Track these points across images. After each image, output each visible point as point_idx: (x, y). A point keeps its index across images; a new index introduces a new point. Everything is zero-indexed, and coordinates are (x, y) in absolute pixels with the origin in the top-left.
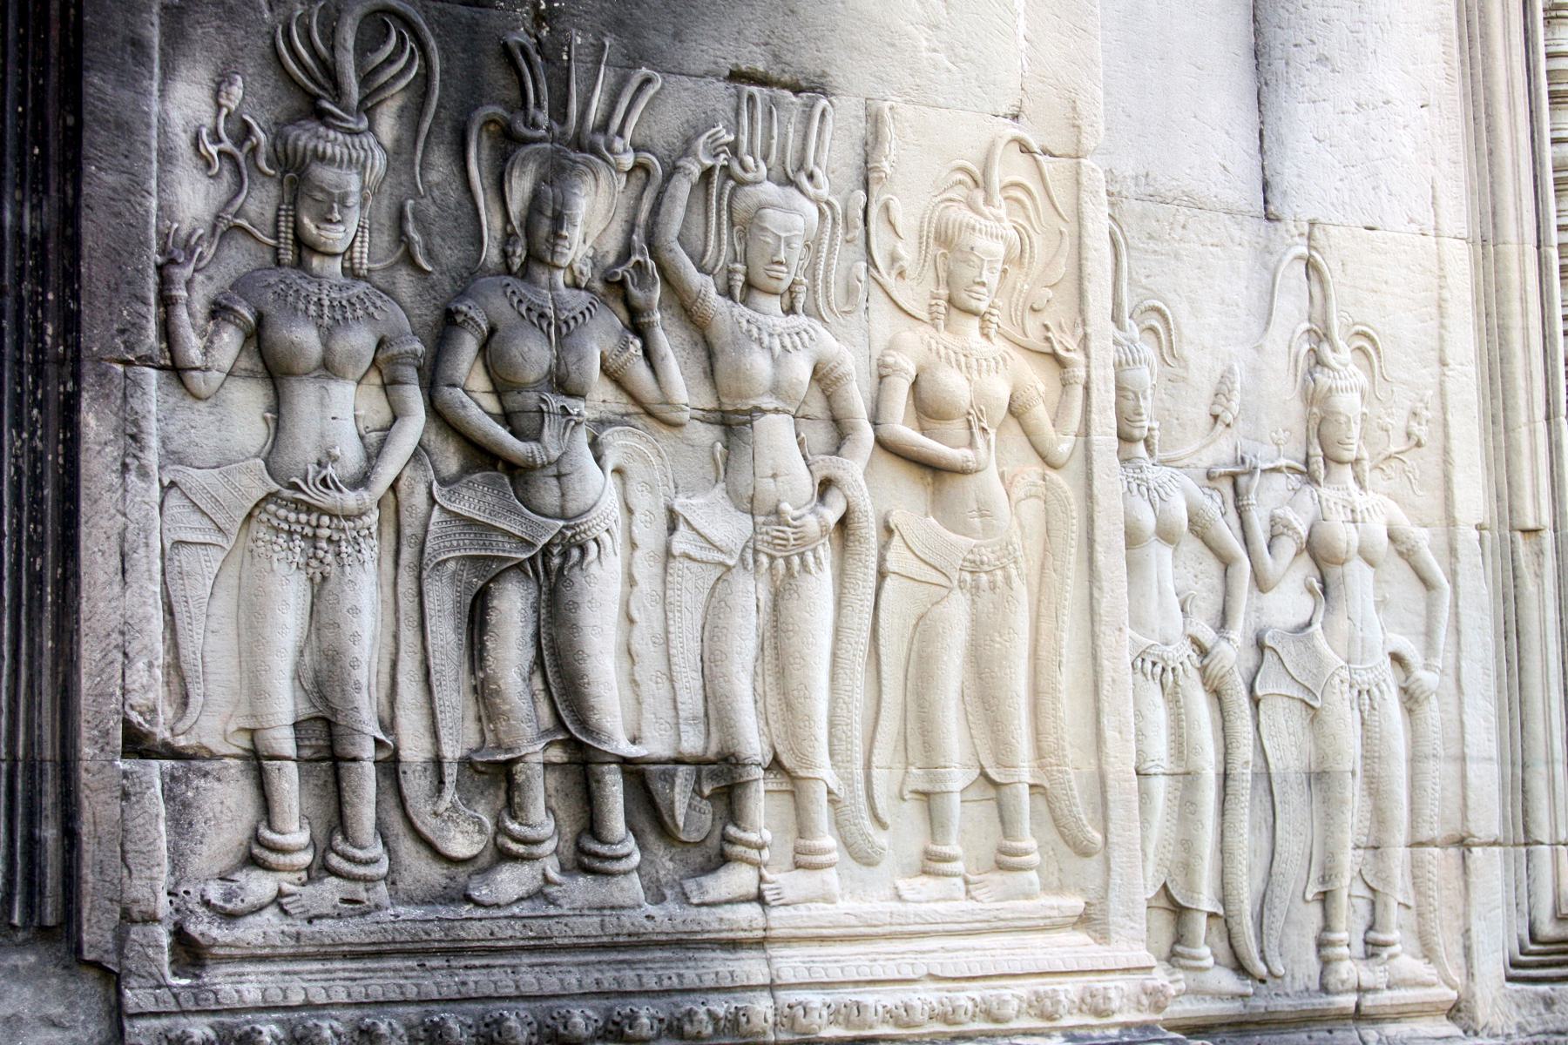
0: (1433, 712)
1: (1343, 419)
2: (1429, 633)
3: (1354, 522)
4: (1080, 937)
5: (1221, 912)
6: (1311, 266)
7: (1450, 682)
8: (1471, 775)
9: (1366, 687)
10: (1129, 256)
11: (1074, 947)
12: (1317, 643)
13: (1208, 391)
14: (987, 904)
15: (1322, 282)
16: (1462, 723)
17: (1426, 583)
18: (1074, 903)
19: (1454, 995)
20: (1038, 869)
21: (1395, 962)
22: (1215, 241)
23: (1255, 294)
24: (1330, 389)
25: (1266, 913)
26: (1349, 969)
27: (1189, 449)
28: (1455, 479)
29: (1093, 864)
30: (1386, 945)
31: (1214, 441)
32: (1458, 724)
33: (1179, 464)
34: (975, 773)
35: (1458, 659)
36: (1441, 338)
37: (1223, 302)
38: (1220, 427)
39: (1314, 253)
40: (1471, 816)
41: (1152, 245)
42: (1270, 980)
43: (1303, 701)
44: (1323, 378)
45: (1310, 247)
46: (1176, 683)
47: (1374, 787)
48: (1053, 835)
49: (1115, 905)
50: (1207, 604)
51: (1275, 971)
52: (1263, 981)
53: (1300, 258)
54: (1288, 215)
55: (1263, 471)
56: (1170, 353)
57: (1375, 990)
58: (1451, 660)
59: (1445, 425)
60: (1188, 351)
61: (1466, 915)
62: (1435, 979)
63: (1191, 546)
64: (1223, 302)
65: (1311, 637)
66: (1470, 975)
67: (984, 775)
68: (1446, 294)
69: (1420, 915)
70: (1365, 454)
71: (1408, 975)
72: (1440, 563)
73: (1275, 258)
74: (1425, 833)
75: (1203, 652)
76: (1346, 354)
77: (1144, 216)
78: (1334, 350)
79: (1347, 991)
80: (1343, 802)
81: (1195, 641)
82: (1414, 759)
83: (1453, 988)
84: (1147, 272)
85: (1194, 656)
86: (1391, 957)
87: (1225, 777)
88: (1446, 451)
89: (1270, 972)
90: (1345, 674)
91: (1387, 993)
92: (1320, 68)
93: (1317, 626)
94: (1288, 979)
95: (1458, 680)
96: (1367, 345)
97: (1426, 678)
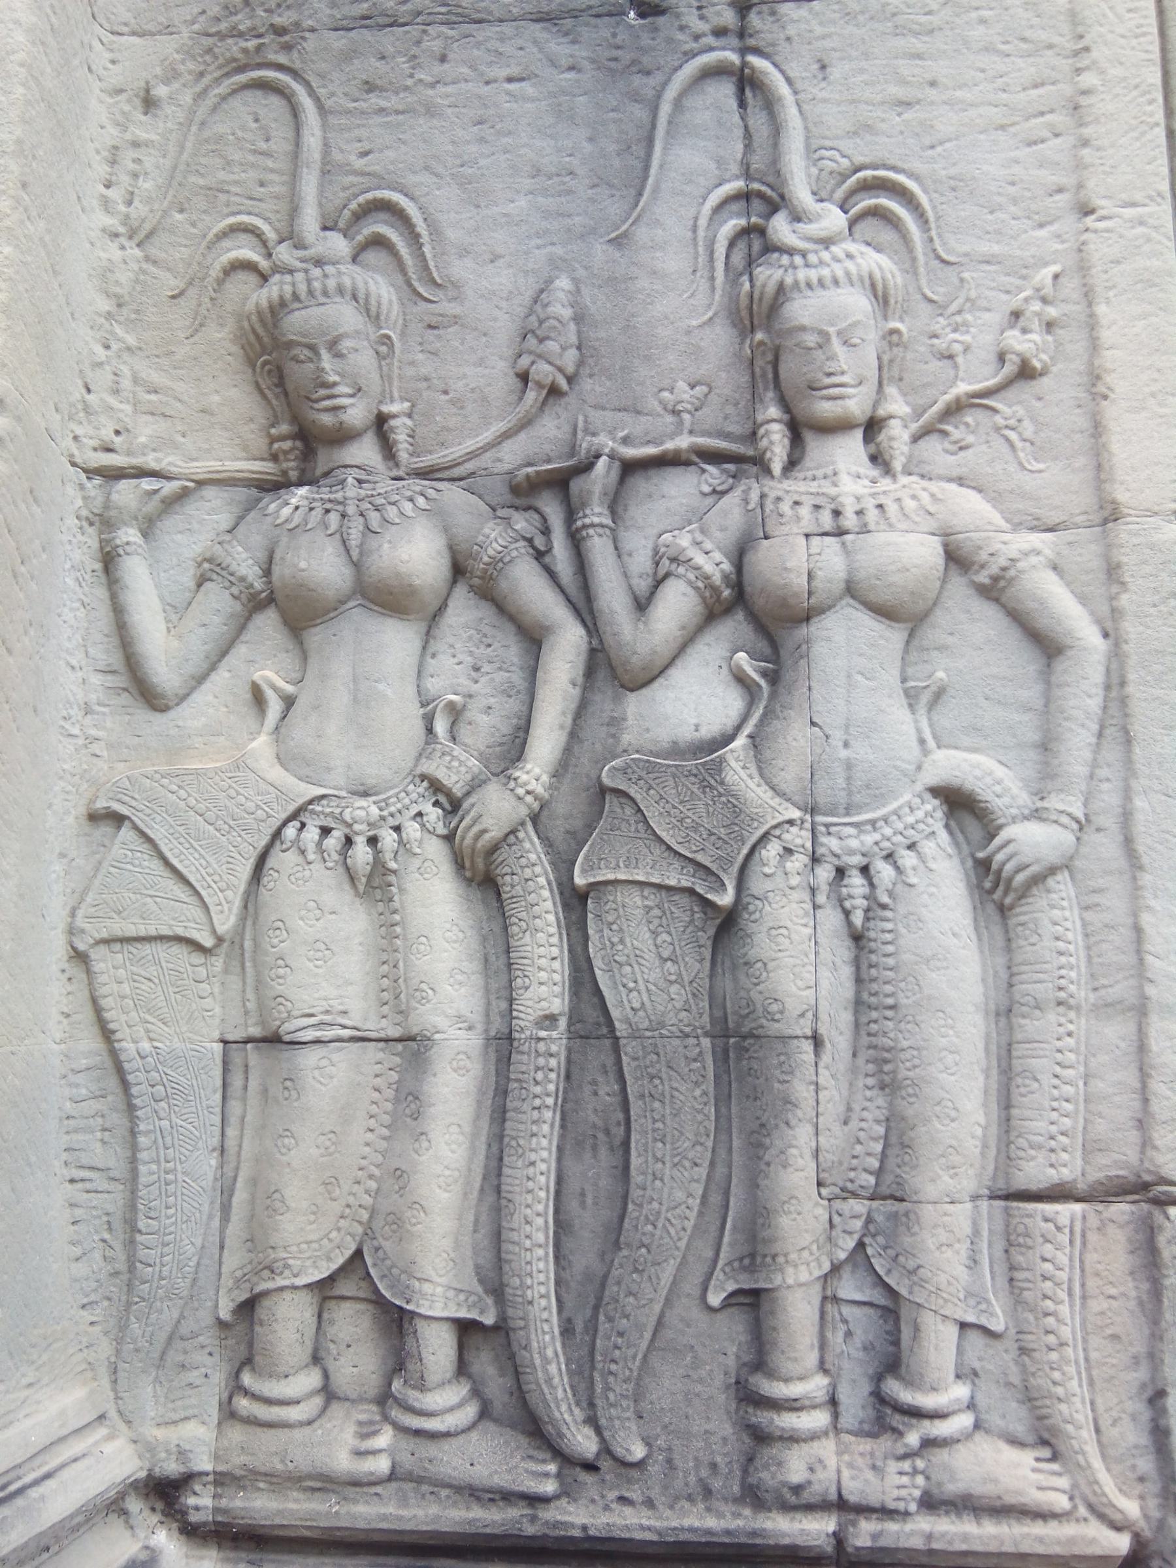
0: (1056, 916)
1: (811, 339)
2: (1046, 746)
3: (840, 533)
5: (489, 1320)
6: (746, 83)
7: (1105, 847)
8: (1156, 1044)
9: (857, 860)
10: (325, 126)
12: (730, 777)
13: (504, 327)
15: (770, 105)
16: (1138, 930)
17: (1046, 645)
19: (1121, 1544)
21: (941, 1456)
22: (514, 71)
23: (612, 148)
24: (781, 288)
25: (603, 1326)
26: (823, 1455)
27: (470, 444)
28: (1112, 425)
30: (917, 1414)
31: (525, 424)
32: (1127, 933)
33: (457, 472)
35: (1127, 794)
36: (1080, 166)
37: (537, 172)
39: (753, 60)
40: (1163, 1137)
41: (375, 100)
42: (605, 1464)
43: (691, 892)
44: (768, 274)
45: (744, 51)
51: (619, 1451)
52: (590, 1467)
56: (422, 282)
58: (1109, 797)
59: (1092, 324)
60: (460, 269)
61: (1154, 1358)
62: (1062, 1502)
63: (463, 612)
64: (537, 172)
65: (719, 766)
68: (1089, 79)
69: (1023, 1351)
70: (896, 405)
71: (978, 1489)
72: (1083, 599)
73: (658, 78)
74: (1035, 1171)
75: (453, 806)
76: (833, 219)
78: (797, 217)
79: (809, 1508)
81: (436, 786)
82: (1006, 1011)
83: (1117, 1528)
84: (366, 146)
85: (433, 814)
87: (503, 1046)
88: (1095, 377)
89: (606, 1450)
90: (799, 837)
91: (924, 1524)
93: (740, 742)
94: (654, 1469)
95: (1128, 842)
96: (875, 198)
97: (1028, 840)
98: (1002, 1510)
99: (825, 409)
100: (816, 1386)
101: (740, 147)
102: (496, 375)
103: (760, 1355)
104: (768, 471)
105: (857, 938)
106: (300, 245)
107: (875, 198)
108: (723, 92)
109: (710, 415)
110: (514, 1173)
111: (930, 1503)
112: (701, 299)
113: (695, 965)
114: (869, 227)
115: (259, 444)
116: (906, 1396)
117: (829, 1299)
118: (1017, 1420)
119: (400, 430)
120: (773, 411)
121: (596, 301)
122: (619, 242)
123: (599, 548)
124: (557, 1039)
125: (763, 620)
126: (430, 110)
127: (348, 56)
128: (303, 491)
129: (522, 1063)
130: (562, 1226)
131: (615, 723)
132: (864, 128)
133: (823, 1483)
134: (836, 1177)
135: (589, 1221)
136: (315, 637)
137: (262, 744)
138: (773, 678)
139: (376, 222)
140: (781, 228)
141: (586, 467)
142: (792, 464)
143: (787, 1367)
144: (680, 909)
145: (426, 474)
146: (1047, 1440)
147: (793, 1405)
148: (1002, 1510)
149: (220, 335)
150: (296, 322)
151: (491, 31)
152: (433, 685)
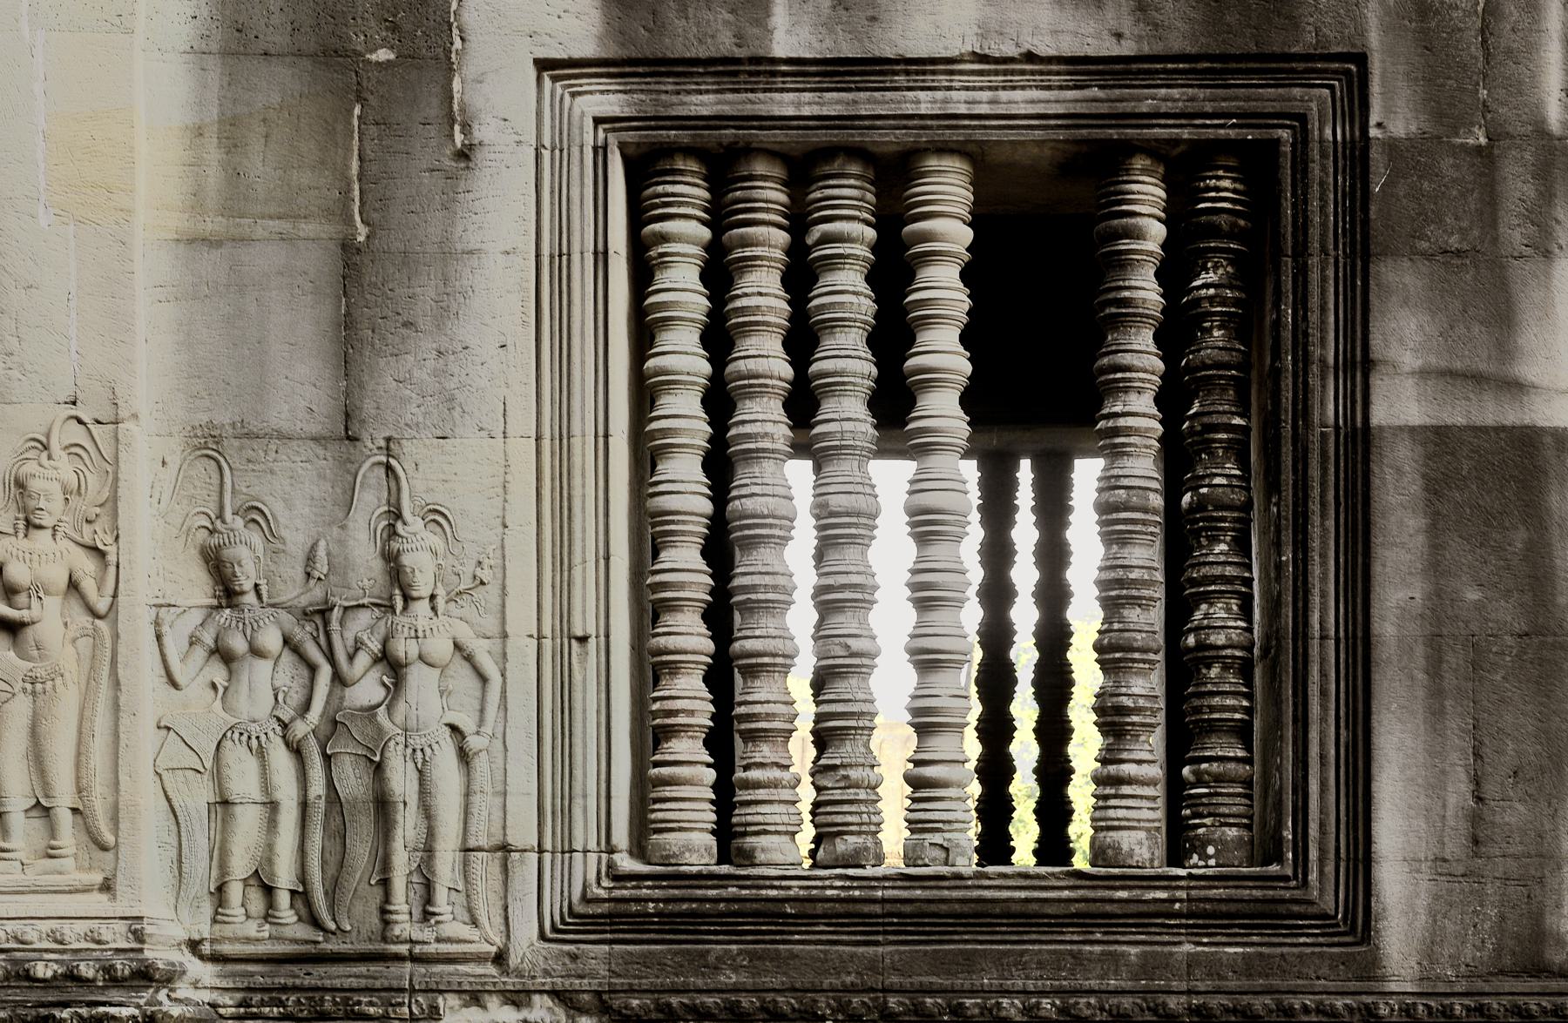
4: (104, 897)
6: (389, 468)
11: (97, 903)
13: (301, 557)
14: (30, 878)
15: (397, 478)
18: (98, 878)
19: (494, 949)
20: (75, 856)
23: (339, 491)
29: (109, 856)
30: (434, 914)
34: (33, 801)
38: (312, 582)
46: (260, 744)
47: (427, 812)
48: (85, 838)
49: (120, 878)
50: (296, 698)
53: (379, 463)
54: (365, 436)
55: (346, 608)
56: (271, 535)
57: (424, 943)
60: (284, 533)
63: (288, 658)
66: (508, 937)
67: (38, 802)
74: (472, 843)
77: (241, 448)
80: (395, 822)
85: (278, 729)
86: (438, 922)
87: (304, 805)
92: (404, 331)
96: (435, 516)
98: (459, 941)
99: (415, 594)
100: (405, 908)
101: (386, 494)
102: (299, 573)
103: (387, 897)
104: (394, 612)
105: (420, 772)
106: (224, 522)
107: (435, 516)
108: (382, 471)
109: (376, 591)
110: (309, 845)
111: (438, 940)
112: (372, 549)
113: (367, 779)
114: (432, 526)
115: (210, 591)
116: (431, 909)
117: (409, 882)
118: (466, 918)
119: (264, 590)
120: (397, 591)
121: (335, 549)
122: (343, 527)
123: (336, 638)
124: (322, 803)
125: (392, 666)
126: (272, 472)
127: (241, 448)
128: (228, 611)
129: (310, 810)
130: (324, 862)
131: (342, 698)
132: (429, 490)
133: (405, 935)
134: (411, 845)
135: (333, 860)
136: (234, 665)
137: (218, 703)
138: (396, 685)
139: (254, 514)
140: (399, 526)
141: (332, 609)
142: (405, 608)
143: (394, 900)
144: (362, 762)
145: (273, 606)
146: (474, 922)
147: (396, 912)
148: (459, 941)
149: (194, 553)
150: (227, 553)
151: (295, 443)
152: (277, 684)
